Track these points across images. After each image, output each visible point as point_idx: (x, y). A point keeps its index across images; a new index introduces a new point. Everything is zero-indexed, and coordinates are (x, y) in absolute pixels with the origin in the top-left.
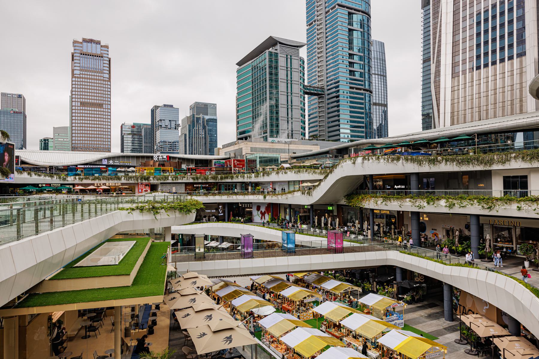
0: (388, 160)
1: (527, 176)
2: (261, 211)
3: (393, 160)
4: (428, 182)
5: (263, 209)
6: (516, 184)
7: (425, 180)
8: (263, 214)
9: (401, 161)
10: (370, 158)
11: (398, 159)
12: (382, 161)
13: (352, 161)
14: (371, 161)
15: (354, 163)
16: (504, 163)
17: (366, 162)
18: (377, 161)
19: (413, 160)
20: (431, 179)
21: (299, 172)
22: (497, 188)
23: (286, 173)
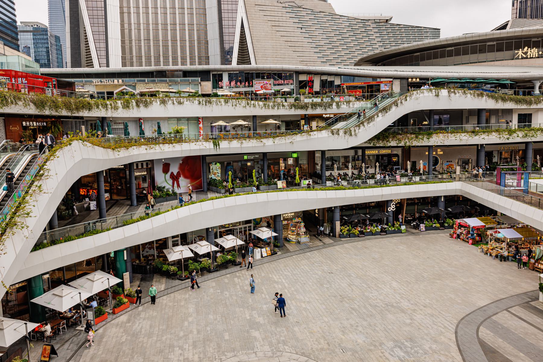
0: (474, 96)
1: (530, 115)
2: (172, 173)
3: (478, 95)
4: (440, 119)
5: (174, 169)
6: (525, 119)
7: (436, 117)
8: (175, 178)
9: (484, 97)
10: (456, 91)
11: (482, 95)
12: (469, 95)
13: (434, 94)
14: (457, 95)
15: (437, 95)
16: (537, 104)
17: (453, 95)
18: (464, 96)
19: (492, 97)
20: (445, 116)
21: (210, 102)
22: (515, 123)
23: (180, 103)
